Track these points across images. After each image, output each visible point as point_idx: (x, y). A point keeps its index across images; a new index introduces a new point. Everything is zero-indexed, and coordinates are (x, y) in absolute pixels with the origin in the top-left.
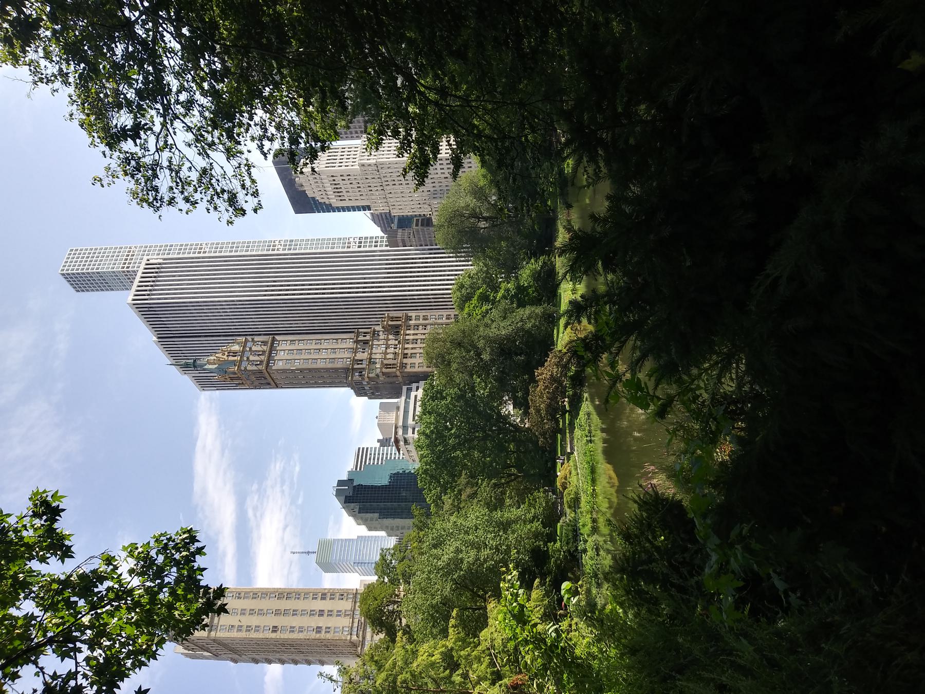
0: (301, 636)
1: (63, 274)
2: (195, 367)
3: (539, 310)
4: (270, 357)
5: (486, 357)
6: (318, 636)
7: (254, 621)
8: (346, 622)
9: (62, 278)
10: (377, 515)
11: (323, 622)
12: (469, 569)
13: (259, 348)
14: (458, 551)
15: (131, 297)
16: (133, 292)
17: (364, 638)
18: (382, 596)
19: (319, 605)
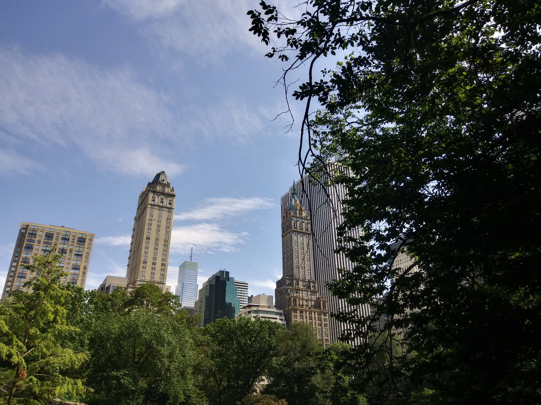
0: (143, 253)
4: (299, 232)
5: (296, 365)
6: (142, 262)
7: (154, 228)
10: (208, 294)
11: (149, 265)
12: (159, 351)
13: (304, 226)
14: (169, 343)
18: (152, 297)
19: (159, 262)
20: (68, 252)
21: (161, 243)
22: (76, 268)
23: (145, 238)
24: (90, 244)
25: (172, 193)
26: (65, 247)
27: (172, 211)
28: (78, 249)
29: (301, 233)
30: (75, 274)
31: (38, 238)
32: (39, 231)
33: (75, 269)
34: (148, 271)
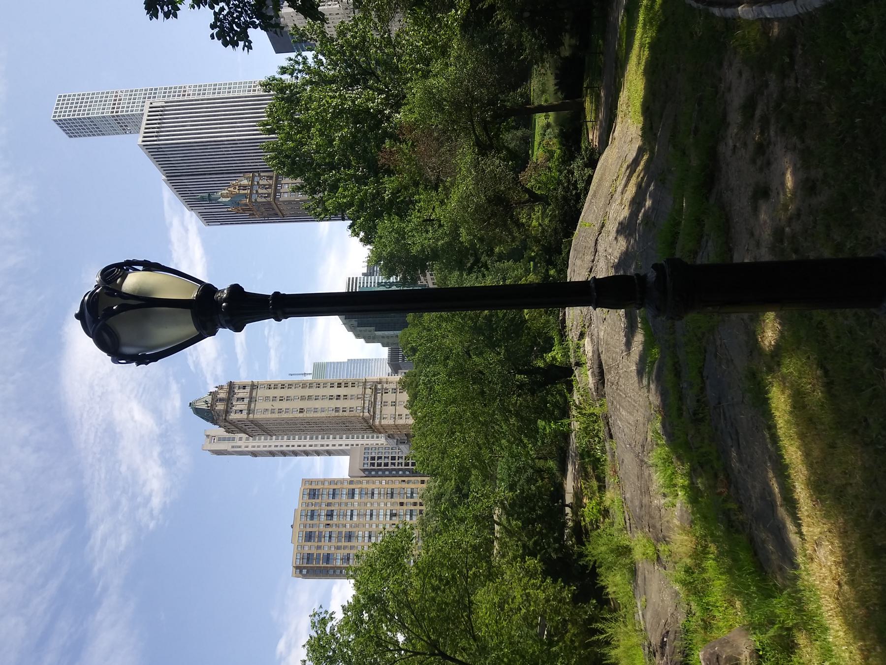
0: (323, 415)
2: (210, 200)
4: (276, 191)
6: (337, 414)
7: (284, 405)
8: (359, 403)
9: (55, 124)
10: (373, 328)
11: (340, 404)
15: (141, 139)
16: (142, 134)
17: (374, 413)
19: (336, 391)
20: (330, 508)
21: (307, 392)
22: (352, 494)
23: (301, 415)
24: (317, 482)
27: (256, 383)
28: (325, 496)
29: (276, 187)
30: (360, 494)
31: (314, 551)
32: (302, 552)
34: (347, 404)
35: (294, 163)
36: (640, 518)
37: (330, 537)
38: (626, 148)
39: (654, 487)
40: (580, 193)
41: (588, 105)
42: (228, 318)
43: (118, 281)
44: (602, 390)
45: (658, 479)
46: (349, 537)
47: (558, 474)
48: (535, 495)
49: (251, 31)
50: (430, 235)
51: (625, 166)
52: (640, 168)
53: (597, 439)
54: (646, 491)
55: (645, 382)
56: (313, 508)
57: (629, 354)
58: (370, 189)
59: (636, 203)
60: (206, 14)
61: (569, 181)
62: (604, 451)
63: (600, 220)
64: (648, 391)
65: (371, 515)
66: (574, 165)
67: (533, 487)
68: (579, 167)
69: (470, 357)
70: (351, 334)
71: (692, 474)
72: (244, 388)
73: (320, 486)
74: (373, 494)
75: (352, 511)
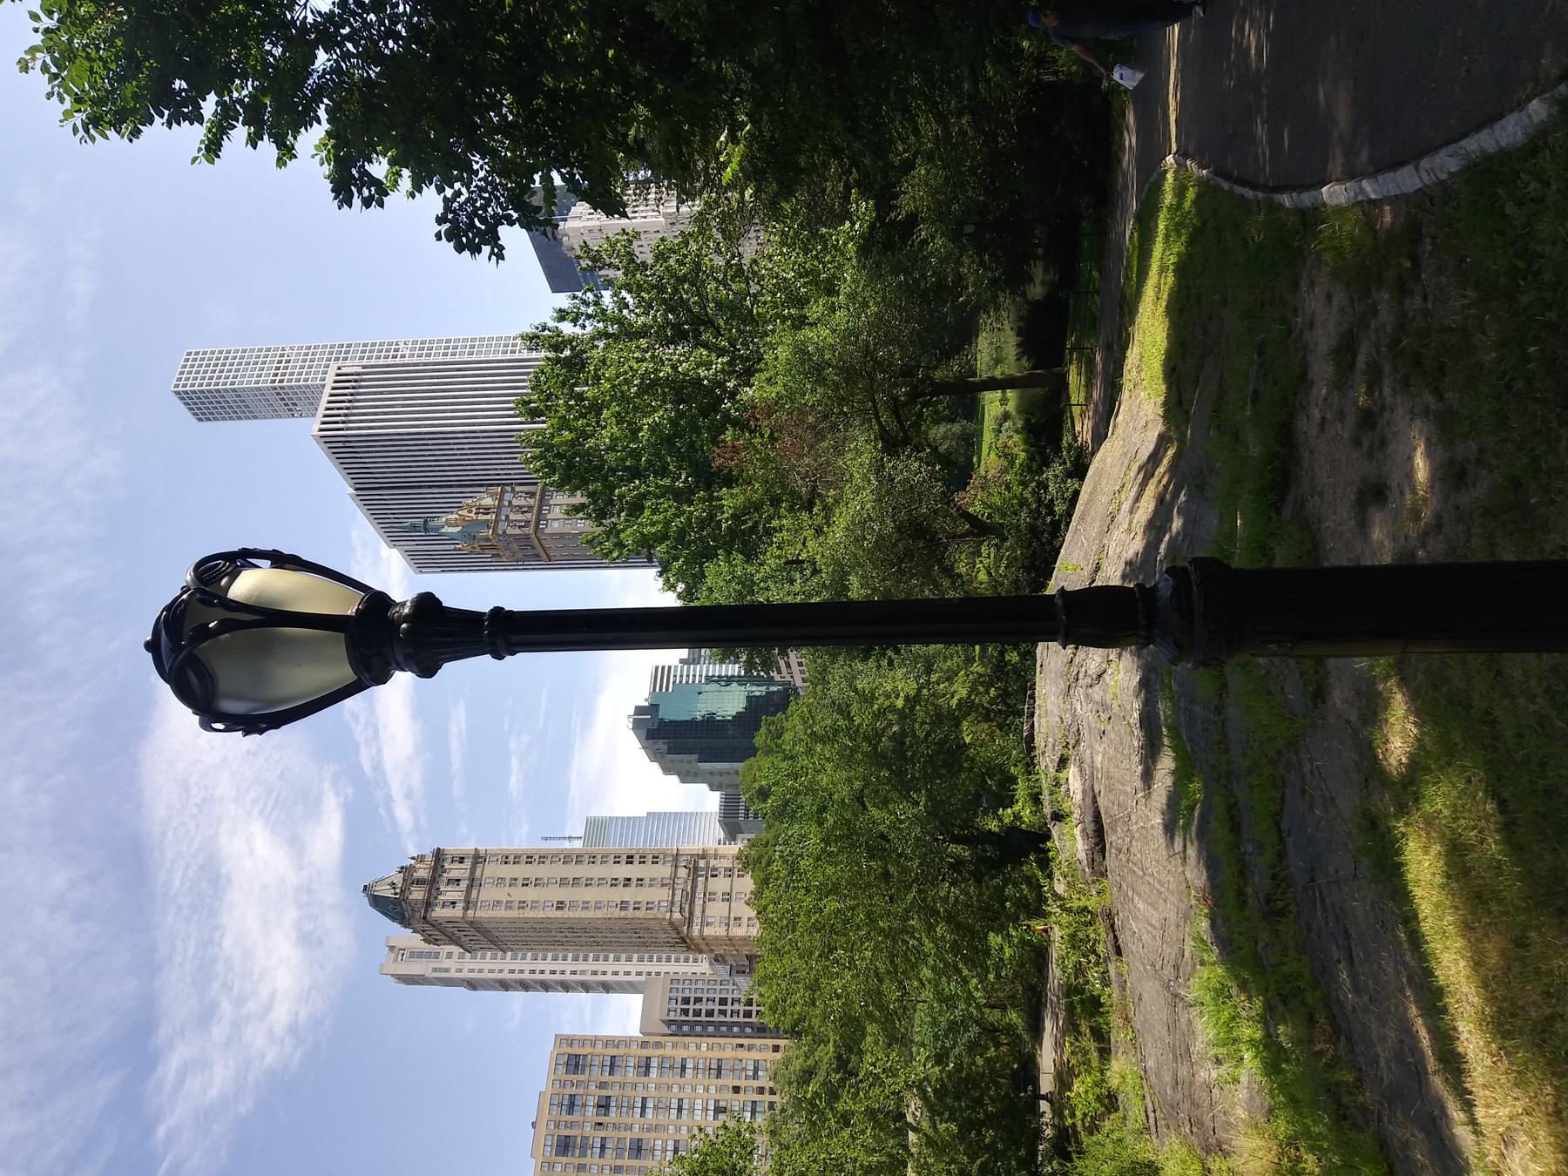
0: (599, 914)
1: (178, 393)
2: (426, 530)
3: (957, 428)
6: (623, 913)
7: (530, 894)
8: (663, 894)
9: (175, 398)
11: (629, 895)
13: (522, 502)
15: (317, 426)
17: (691, 914)
19: (623, 871)
20: (604, 1093)
21: (572, 871)
23: (559, 914)
24: (583, 1041)
25: (429, 858)
26: (592, 1101)
27: (482, 853)
29: (540, 509)
30: (661, 1067)
33: (648, 1067)
35: (570, 466)
36: (1175, 1107)
37: (603, 1148)
38: (1136, 438)
39: (1199, 1046)
40: (1059, 521)
41: (1074, 378)
42: (410, 650)
43: (223, 582)
44: (1101, 864)
45: (1205, 1029)
46: (638, 1149)
47: (1026, 1037)
48: (982, 1076)
49: (504, 231)
50: (797, 587)
51: (1135, 467)
52: (1161, 469)
53: (1092, 958)
54: (1183, 1053)
55: (1178, 842)
56: (573, 1091)
57: (1148, 796)
58: (696, 510)
59: (1156, 526)
60: (431, 200)
61: (1039, 501)
62: (1106, 982)
63: (1093, 559)
64: (1184, 859)
65: (680, 1109)
66: (1048, 474)
67: (980, 1061)
68: (1056, 476)
69: (865, 808)
70: (655, 767)
71: (1268, 1018)
72: (462, 860)
73: (587, 1050)
74: (683, 1068)
75: (644, 1099)
